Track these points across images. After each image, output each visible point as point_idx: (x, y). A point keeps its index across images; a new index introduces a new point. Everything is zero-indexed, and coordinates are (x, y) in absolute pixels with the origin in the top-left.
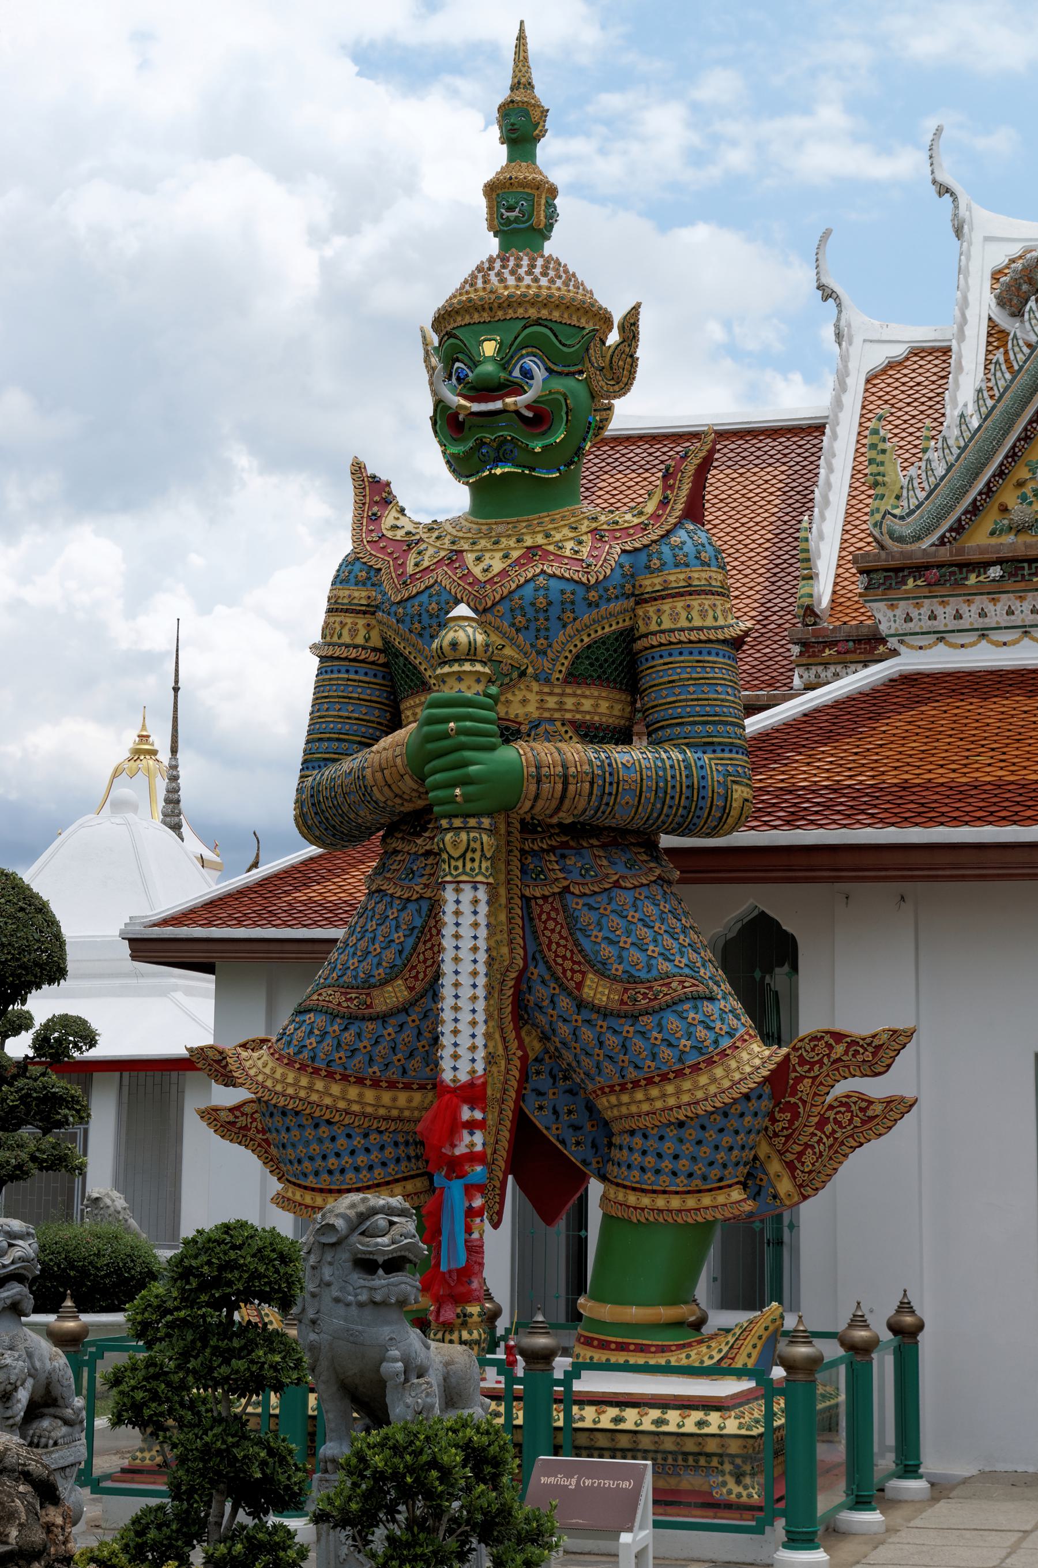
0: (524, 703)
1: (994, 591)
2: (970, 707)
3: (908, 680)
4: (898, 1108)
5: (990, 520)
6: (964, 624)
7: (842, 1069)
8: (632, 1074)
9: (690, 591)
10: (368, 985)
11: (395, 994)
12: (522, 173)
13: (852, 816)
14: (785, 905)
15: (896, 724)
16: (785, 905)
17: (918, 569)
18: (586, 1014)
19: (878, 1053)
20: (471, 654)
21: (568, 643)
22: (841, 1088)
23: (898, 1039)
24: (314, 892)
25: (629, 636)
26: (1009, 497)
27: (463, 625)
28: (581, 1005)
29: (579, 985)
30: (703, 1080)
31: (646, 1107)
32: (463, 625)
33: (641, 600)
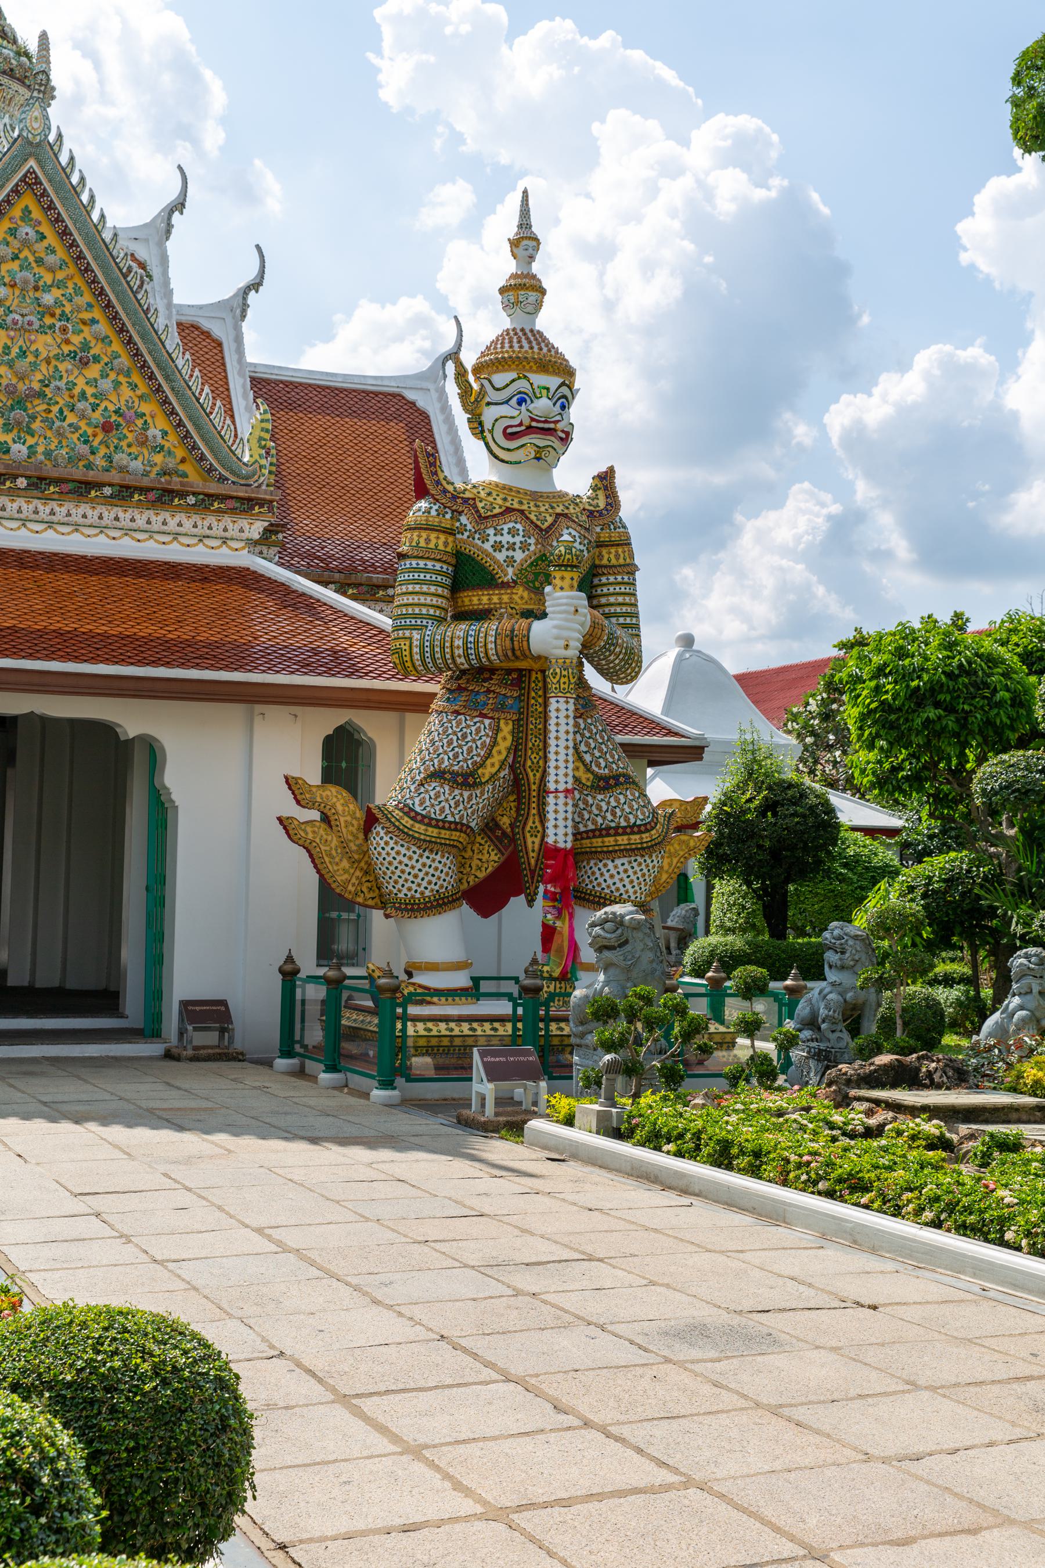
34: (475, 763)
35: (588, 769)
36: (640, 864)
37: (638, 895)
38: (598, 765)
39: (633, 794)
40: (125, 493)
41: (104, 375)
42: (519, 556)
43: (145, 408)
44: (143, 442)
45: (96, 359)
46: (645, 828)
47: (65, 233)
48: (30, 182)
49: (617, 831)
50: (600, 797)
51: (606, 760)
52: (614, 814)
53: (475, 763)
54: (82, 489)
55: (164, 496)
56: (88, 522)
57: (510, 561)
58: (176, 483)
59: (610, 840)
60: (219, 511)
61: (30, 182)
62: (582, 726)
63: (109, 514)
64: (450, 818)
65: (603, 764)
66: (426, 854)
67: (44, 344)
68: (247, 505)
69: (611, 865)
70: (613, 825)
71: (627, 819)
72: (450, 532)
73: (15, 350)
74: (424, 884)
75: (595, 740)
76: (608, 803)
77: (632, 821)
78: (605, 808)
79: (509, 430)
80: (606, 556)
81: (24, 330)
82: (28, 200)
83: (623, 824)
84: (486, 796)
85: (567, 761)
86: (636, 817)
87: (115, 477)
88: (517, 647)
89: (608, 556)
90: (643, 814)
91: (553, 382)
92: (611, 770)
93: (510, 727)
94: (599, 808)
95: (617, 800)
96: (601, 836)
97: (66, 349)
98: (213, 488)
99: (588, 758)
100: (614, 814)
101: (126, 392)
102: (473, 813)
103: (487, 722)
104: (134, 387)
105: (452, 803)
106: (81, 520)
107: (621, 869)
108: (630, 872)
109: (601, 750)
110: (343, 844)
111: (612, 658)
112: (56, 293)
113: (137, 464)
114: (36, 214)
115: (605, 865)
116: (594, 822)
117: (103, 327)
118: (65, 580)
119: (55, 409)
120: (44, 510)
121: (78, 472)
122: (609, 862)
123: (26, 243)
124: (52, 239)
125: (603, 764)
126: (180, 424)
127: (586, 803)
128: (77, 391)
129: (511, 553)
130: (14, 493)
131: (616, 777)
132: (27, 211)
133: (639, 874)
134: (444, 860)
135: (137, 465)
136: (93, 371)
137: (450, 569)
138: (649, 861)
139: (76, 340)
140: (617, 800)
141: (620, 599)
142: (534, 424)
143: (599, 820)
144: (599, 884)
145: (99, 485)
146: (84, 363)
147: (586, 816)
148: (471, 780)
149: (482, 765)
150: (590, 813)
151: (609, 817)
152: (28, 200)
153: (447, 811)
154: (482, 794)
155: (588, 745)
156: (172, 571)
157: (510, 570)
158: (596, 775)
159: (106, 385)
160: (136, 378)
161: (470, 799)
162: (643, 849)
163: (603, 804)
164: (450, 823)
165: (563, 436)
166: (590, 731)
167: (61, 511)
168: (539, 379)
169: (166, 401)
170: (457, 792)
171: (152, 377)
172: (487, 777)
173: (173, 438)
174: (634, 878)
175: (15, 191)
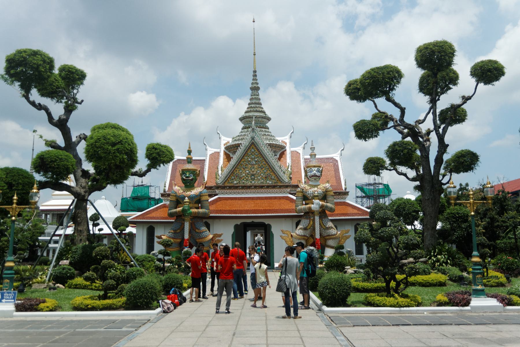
0: (191, 205)
1: (228, 189)
2: (226, 201)
3: (219, 198)
4: (222, 240)
5: (227, 182)
7: (217, 237)
9: (205, 195)
10: (176, 230)
11: (179, 231)
12: (190, 156)
13: (217, 213)
14: (209, 221)
15: (219, 203)
16: (209, 221)
17: (220, 187)
19: (220, 236)
20: (188, 202)
21: (195, 200)
22: (217, 239)
23: (222, 234)
24: (149, 216)
25: (200, 199)
27: (187, 199)
32: (187, 199)
33: (201, 196)
40: (268, 187)
44: (271, 179)
46: (335, 235)
48: (253, 143)
54: (262, 187)
55: (274, 187)
58: (275, 184)
61: (253, 143)
63: (266, 190)
68: (287, 187)
72: (302, 192)
81: (253, 164)
82: (253, 146)
87: (266, 185)
88: (310, 208)
89: (328, 193)
91: (316, 169)
98: (281, 184)
101: (269, 172)
110: (290, 239)
113: (270, 182)
117: (264, 163)
118: (258, 201)
120: (257, 191)
121: (261, 185)
123: (253, 152)
124: (256, 151)
130: (252, 189)
135: (270, 182)
136: (264, 169)
145: (264, 186)
146: (262, 168)
152: (253, 146)
156: (275, 198)
159: (265, 171)
167: (259, 191)
168: (313, 169)
173: (276, 178)
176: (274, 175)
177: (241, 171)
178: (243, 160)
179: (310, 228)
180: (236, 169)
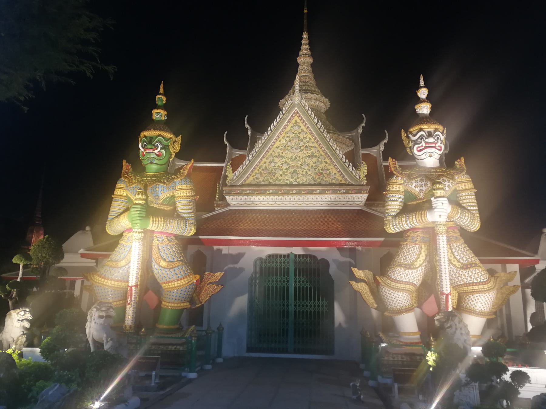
6: (242, 200)
8: (168, 280)
18: (161, 268)
26: (251, 178)
28: (160, 266)
29: (159, 263)
30: (182, 281)
31: (171, 286)
34: (413, 261)
35: (458, 261)
36: (484, 297)
37: (485, 308)
38: (463, 260)
39: (478, 270)
41: (318, 161)
42: (424, 188)
43: (329, 167)
45: (316, 156)
47: (306, 125)
49: (473, 284)
50: (464, 271)
51: (466, 258)
52: (471, 277)
53: (413, 261)
56: (314, 200)
57: (421, 190)
59: (470, 288)
60: (351, 193)
62: (455, 246)
64: (405, 280)
65: (465, 259)
66: (396, 293)
67: (301, 154)
69: (472, 297)
70: (471, 282)
71: (476, 280)
73: (294, 157)
74: (397, 303)
75: (461, 251)
76: (468, 274)
77: (479, 280)
78: (467, 275)
79: (419, 149)
80: (461, 186)
82: (296, 118)
83: (475, 281)
84: (419, 272)
85: (444, 258)
86: (481, 278)
90: (484, 277)
92: (468, 261)
93: (426, 247)
94: (464, 275)
95: (472, 272)
96: (467, 286)
97: (307, 155)
99: (458, 257)
100: (471, 277)
101: (324, 164)
102: (414, 278)
103: (417, 246)
104: (326, 162)
105: (405, 275)
106: (312, 200)
107: (476, 298)
108: (480, 300)
109: (463, 254)
111: (464, 221)
112: (304, 140)
114: (298, 121)
115: (470, 297)
116: (463, 281)
119: (305, 171)
122: (471, 296)
124: (303, 127)
125: (465, 259)
126: (339, 171)
127: (459, 274)
128: (310, 165)
129: (421, 188)
131: (471, 264)
132: (296, 121)
133: (485, 300)
134: (404, 295)
137: (402, 196)
138: (488, 295)
139: (310, 152)
140: (472, 272)
141: (468, 201)
142: (427, 145)
143: (465, 280)
144: (468, 304)
147: (460, 279)
148: (412, 267)
149: (416, 261)
150: (461, 277)
151: (469, 279)
152: (296, 118)
153: (403, 278)
154: (417, 271)
155: (458, 252)
157: (422, 194)
158: (462, 264)
160: (327, 160)
161: (412, 273)
162: (485, 291)
163: (466, 274)
164: (405, 282)
165: (439, 148)
166: (459, 247)
169: (335, 165)
170: (407, 271)
171: (331, 159)
172: (418, 265)
173: (338, 174)
174: (482, 302)
175: (292, 116)
176: (335, 171)
177: (273, 164)
178: (277, 144)
179: (420, 265)
180: (265, 160)
